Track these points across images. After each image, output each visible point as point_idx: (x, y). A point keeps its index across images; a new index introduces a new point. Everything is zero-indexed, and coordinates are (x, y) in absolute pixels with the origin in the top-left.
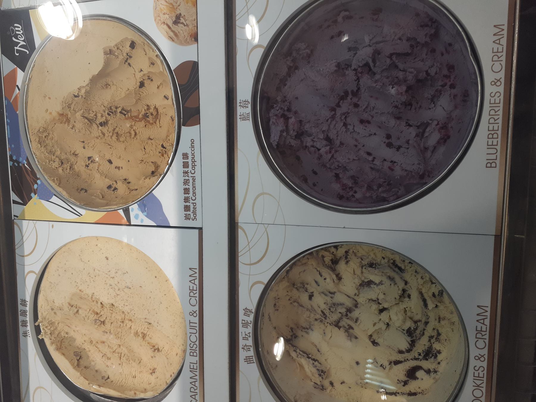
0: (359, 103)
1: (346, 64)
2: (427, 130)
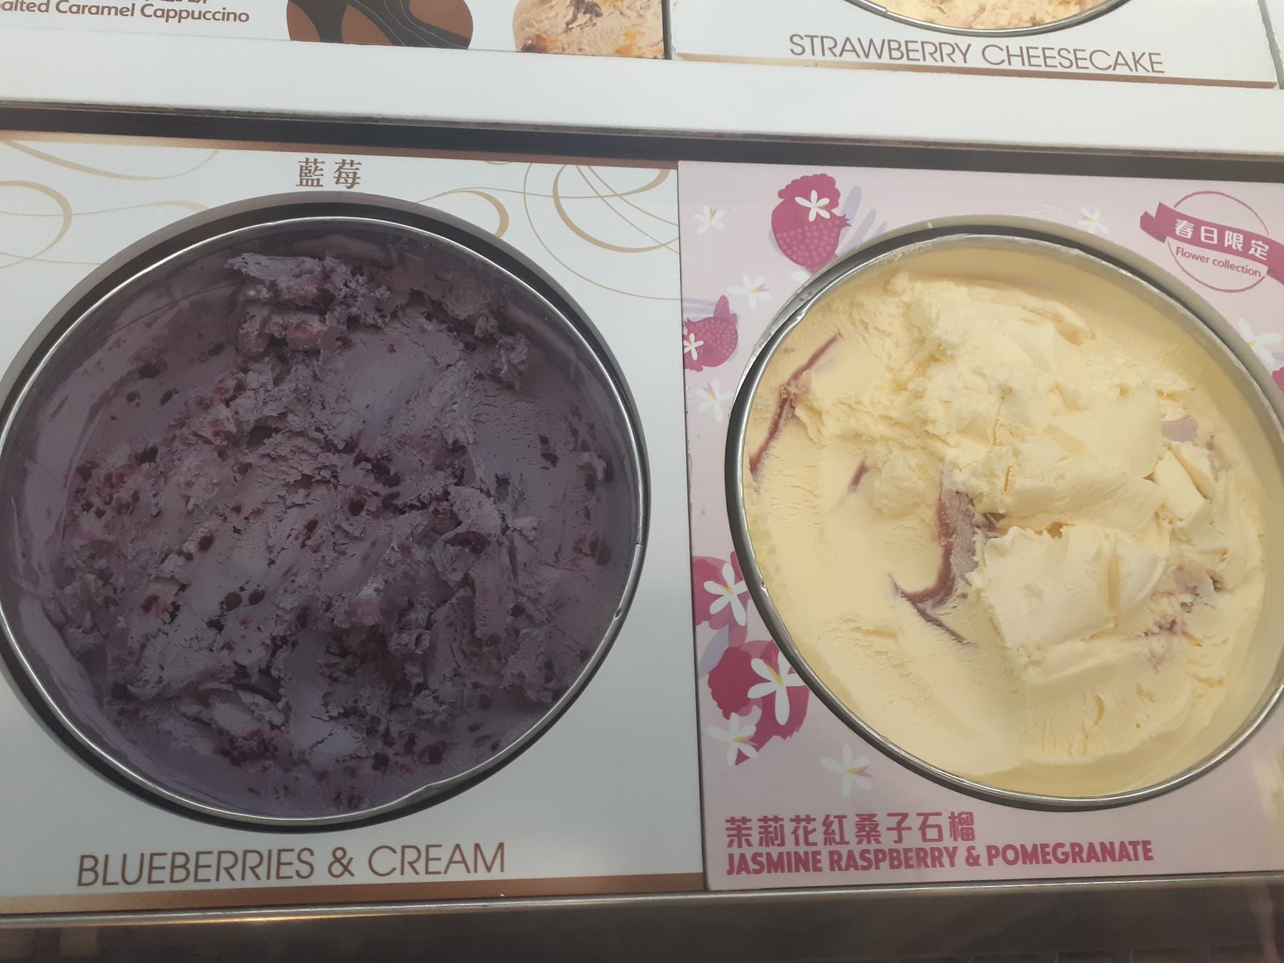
0: (363, 513)
1: (463, 471)
2: (259, 699)
